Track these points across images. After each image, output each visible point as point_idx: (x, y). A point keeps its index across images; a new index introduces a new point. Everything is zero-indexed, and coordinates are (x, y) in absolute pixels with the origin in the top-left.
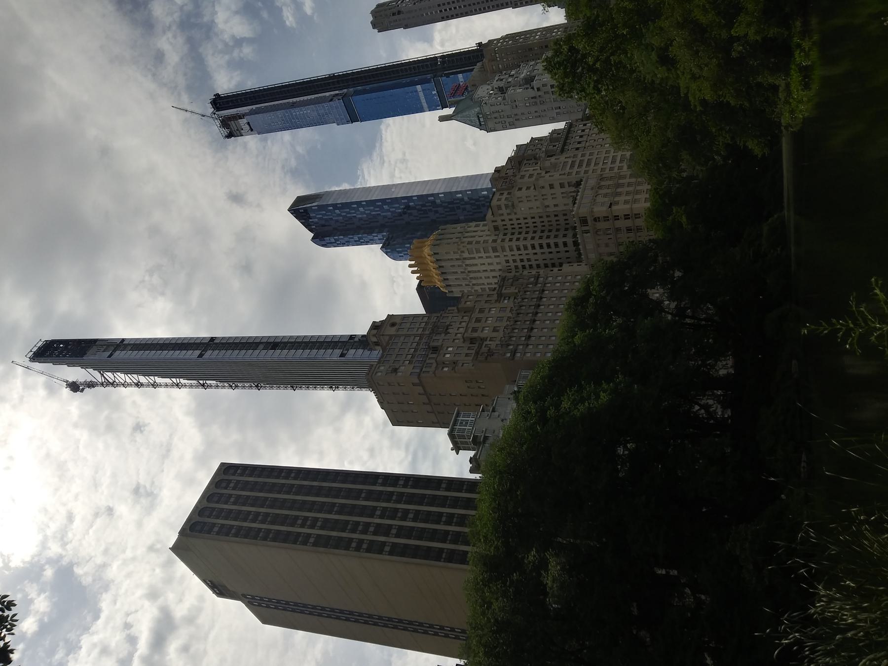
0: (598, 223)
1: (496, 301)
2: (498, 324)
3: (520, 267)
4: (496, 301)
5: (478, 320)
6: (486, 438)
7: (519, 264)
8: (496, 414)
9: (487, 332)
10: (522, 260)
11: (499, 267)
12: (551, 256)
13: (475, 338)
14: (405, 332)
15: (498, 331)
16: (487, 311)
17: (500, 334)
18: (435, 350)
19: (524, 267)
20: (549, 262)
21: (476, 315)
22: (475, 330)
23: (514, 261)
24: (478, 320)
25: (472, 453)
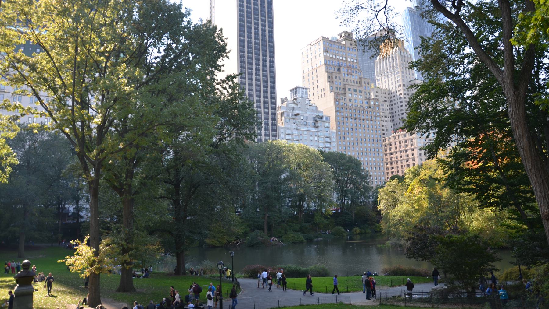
0: (410, 141)
1: (366, 97)
2: (353, 100)
3: (391, 99)
4: (366, 97)
5: (355, 90)
6: (297, 104)
7: (393, 99)
8: (308, 107)
9: (349, 95)
10: (395, 100)
11: (391, 88)
12: (397, 115)
13: (345, 91)
14: (347, 52)
15: (350, 101)
16: (360, 94)
17: (348, 102)
18: (339, 70)
19: (391, 101)
20: (394, 114)
21: (358, 89)
22: (350, 89)
23: (394, 96)
24: (355, 90)
25: (289, 98)
